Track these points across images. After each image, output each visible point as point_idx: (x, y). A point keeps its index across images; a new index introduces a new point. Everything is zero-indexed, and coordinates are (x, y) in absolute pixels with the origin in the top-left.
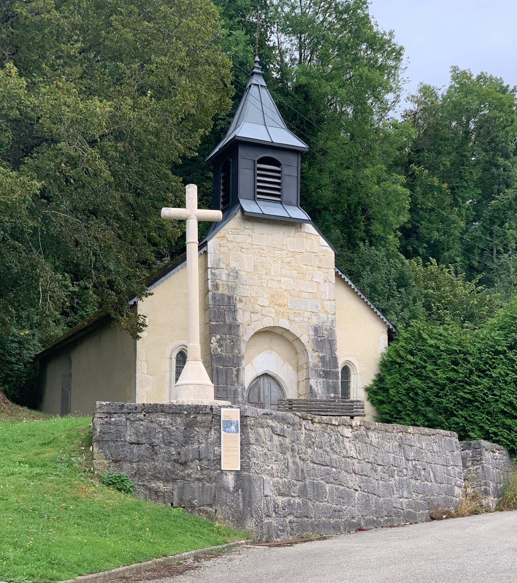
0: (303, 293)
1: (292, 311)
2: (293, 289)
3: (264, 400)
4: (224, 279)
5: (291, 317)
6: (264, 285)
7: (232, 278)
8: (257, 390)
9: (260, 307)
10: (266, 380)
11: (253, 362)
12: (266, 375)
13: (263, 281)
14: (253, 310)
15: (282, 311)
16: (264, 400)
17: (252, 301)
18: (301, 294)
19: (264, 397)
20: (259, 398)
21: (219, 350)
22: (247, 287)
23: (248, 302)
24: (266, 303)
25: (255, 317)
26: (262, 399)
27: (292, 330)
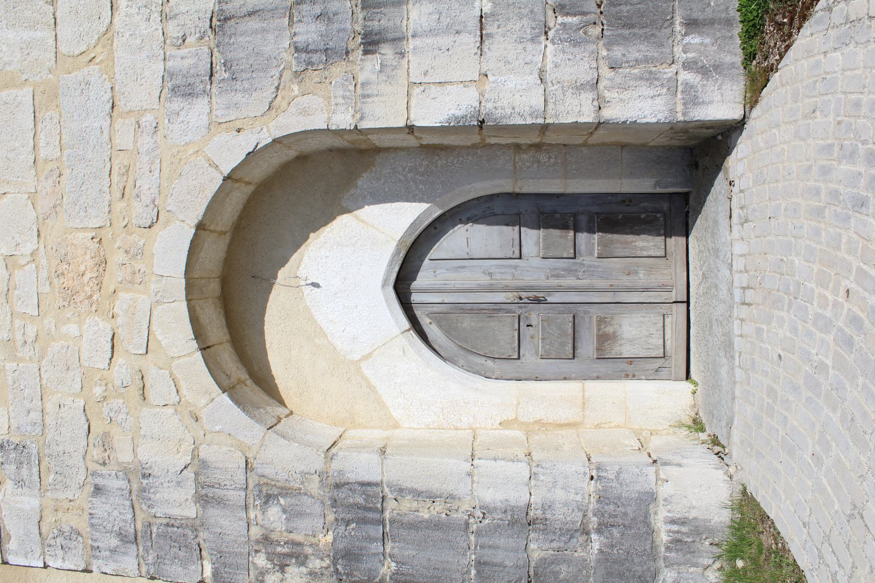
0: (43, 153)
1: (119, 206)
2: (33, 197)
3: (506, 289)
4: (35, 502)
5: (140, 212)
6: (31, 331)
7: (25, 472)
8: (467, 322)
9: (119, 360)
10: (424, 279)
11: (357, 357)
12: (402, 285)
13: (19, 337)
14: (134, 392)
15: (120, 257)
16: (506, 289)
17: (98, 391)
18: (46, 161)
19: (491, 289)
20: (496, 309)
21: (316, 564)
22: (50, 407)
23: (105, 409)
24: (97, 329)
25: (160, 388)
26: (500, 297)
27: (197, 213)
